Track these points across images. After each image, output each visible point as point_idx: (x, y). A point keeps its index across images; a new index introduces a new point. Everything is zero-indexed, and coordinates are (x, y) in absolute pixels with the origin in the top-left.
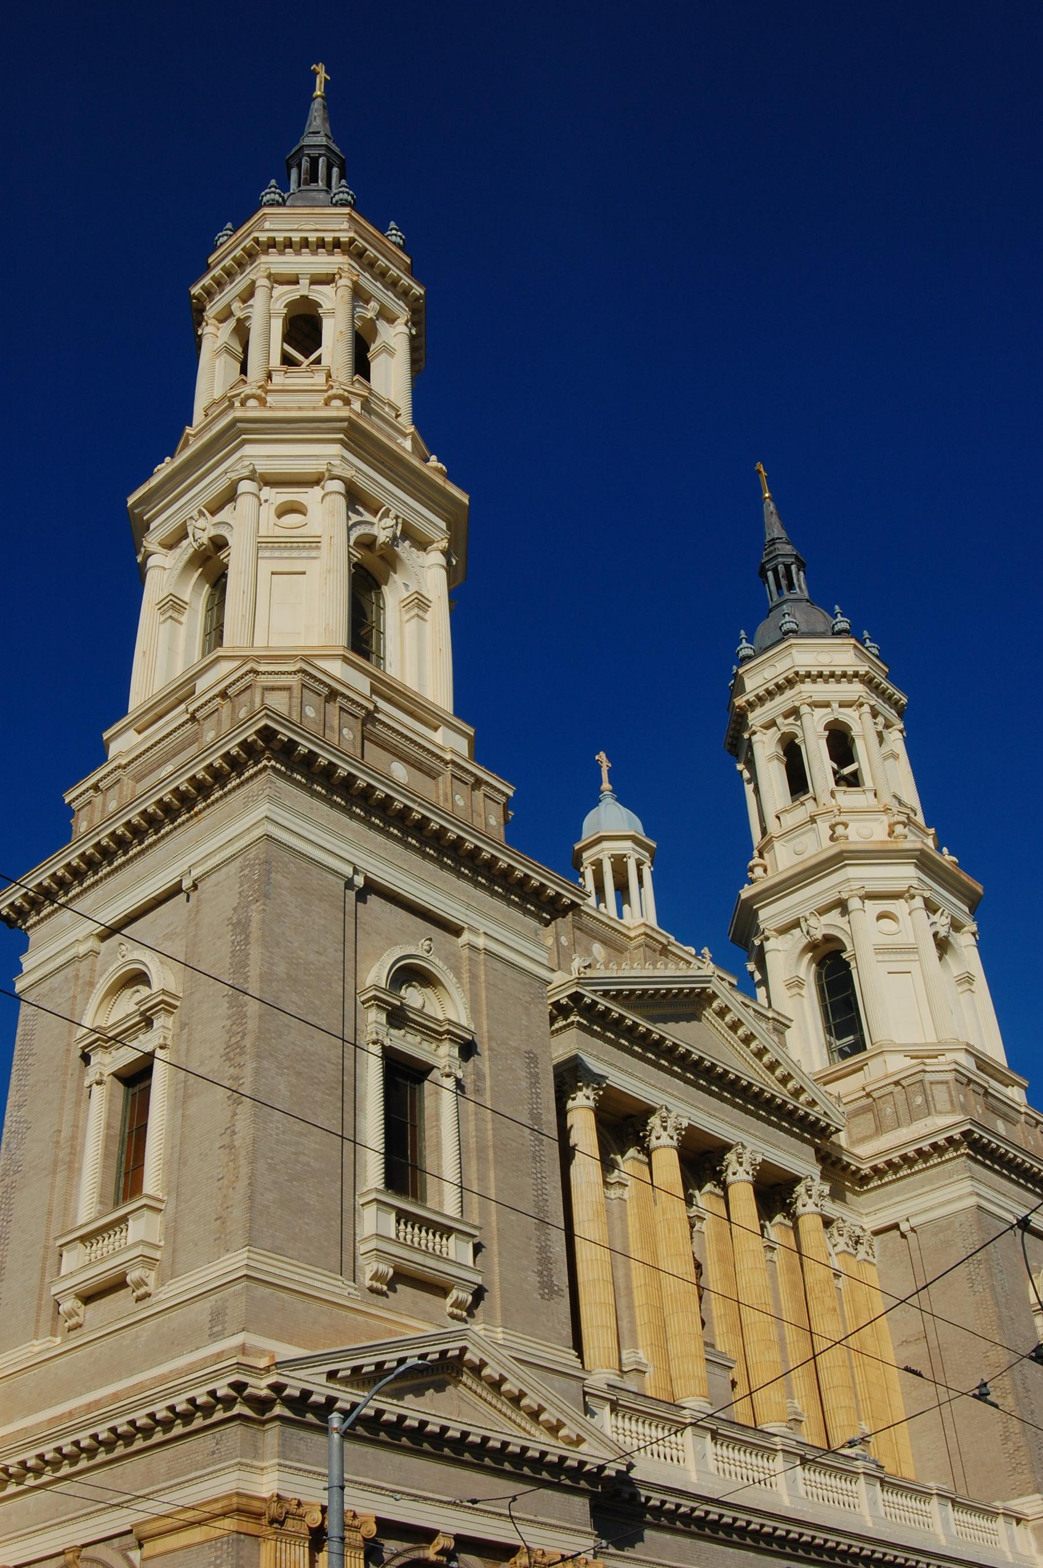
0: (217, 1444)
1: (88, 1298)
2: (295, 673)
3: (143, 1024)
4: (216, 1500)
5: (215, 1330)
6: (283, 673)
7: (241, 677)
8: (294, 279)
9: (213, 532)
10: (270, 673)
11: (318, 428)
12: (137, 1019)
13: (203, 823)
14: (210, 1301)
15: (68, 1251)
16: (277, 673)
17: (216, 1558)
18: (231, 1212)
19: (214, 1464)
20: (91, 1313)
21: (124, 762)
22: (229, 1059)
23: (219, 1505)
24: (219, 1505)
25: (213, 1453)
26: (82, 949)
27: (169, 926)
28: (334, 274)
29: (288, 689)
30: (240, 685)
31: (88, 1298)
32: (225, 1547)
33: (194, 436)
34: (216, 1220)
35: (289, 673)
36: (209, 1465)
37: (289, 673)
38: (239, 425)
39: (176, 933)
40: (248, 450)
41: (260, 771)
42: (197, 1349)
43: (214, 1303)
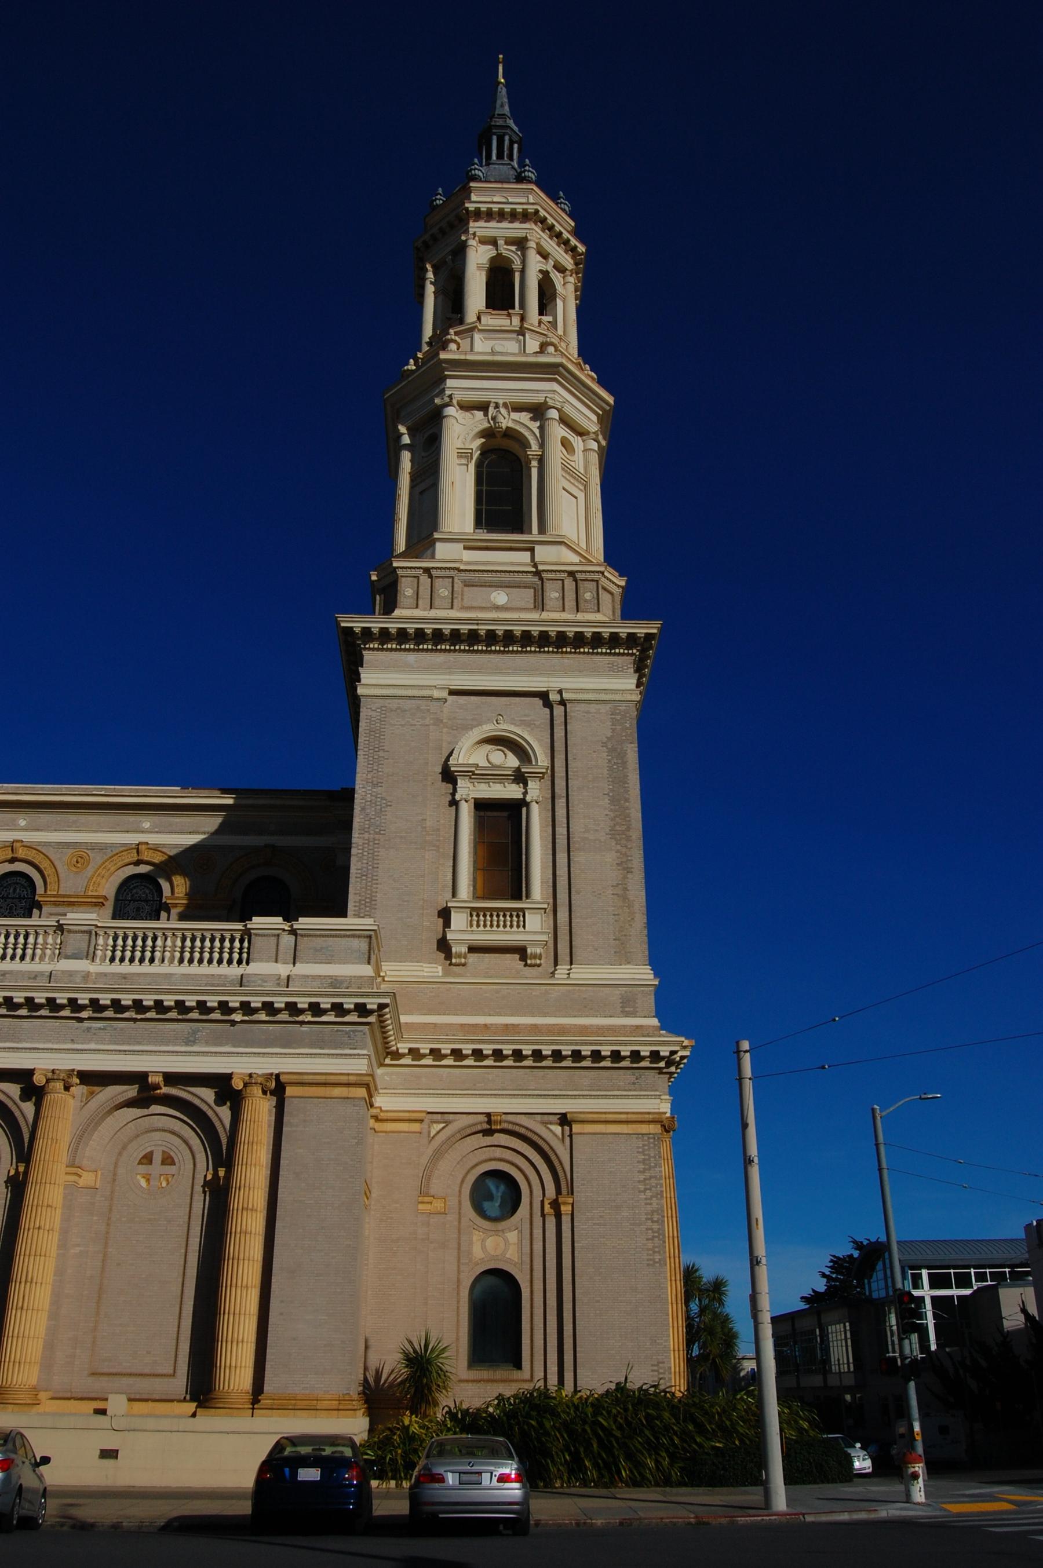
0: (637, 1079)
1: (472, 949)
2: (618, 586)
3: (513, 777)
4: (649, 1113)
5: (627, 1009)
6: (613, 583)
7: (593, 572)
8: (545, 254)
9: (511, 425)
10: (608, 579)
11: (595, 400)
12: (510, 773)
13: (566, 661)
14: (619, 990)
15: (455, 912)
16: (611, 581)
17: (644, 1145)
18: (630, 940)
19: (635, 1090)
20: (473, 958)
21: (462, 567)
22: (616, 839)
23: (651, 1116)
24: (651, 1116)
25: (634, 1083)
26: (436, 694)
27: (525, 715)
28: (567, 269)
29: (611, 594)
30: (588, 576)
31: (472, 949)
32: (652, 1140)
33: (479, 330)
34: (614, 940)
35: (616, 585)
36: (630, 1090)
37: (616, 585)
38: (561, 368)
39: (535, 724)
40: (555, 386)
41: (628, 654)
42: (611, 1017)
43: (623, 992)
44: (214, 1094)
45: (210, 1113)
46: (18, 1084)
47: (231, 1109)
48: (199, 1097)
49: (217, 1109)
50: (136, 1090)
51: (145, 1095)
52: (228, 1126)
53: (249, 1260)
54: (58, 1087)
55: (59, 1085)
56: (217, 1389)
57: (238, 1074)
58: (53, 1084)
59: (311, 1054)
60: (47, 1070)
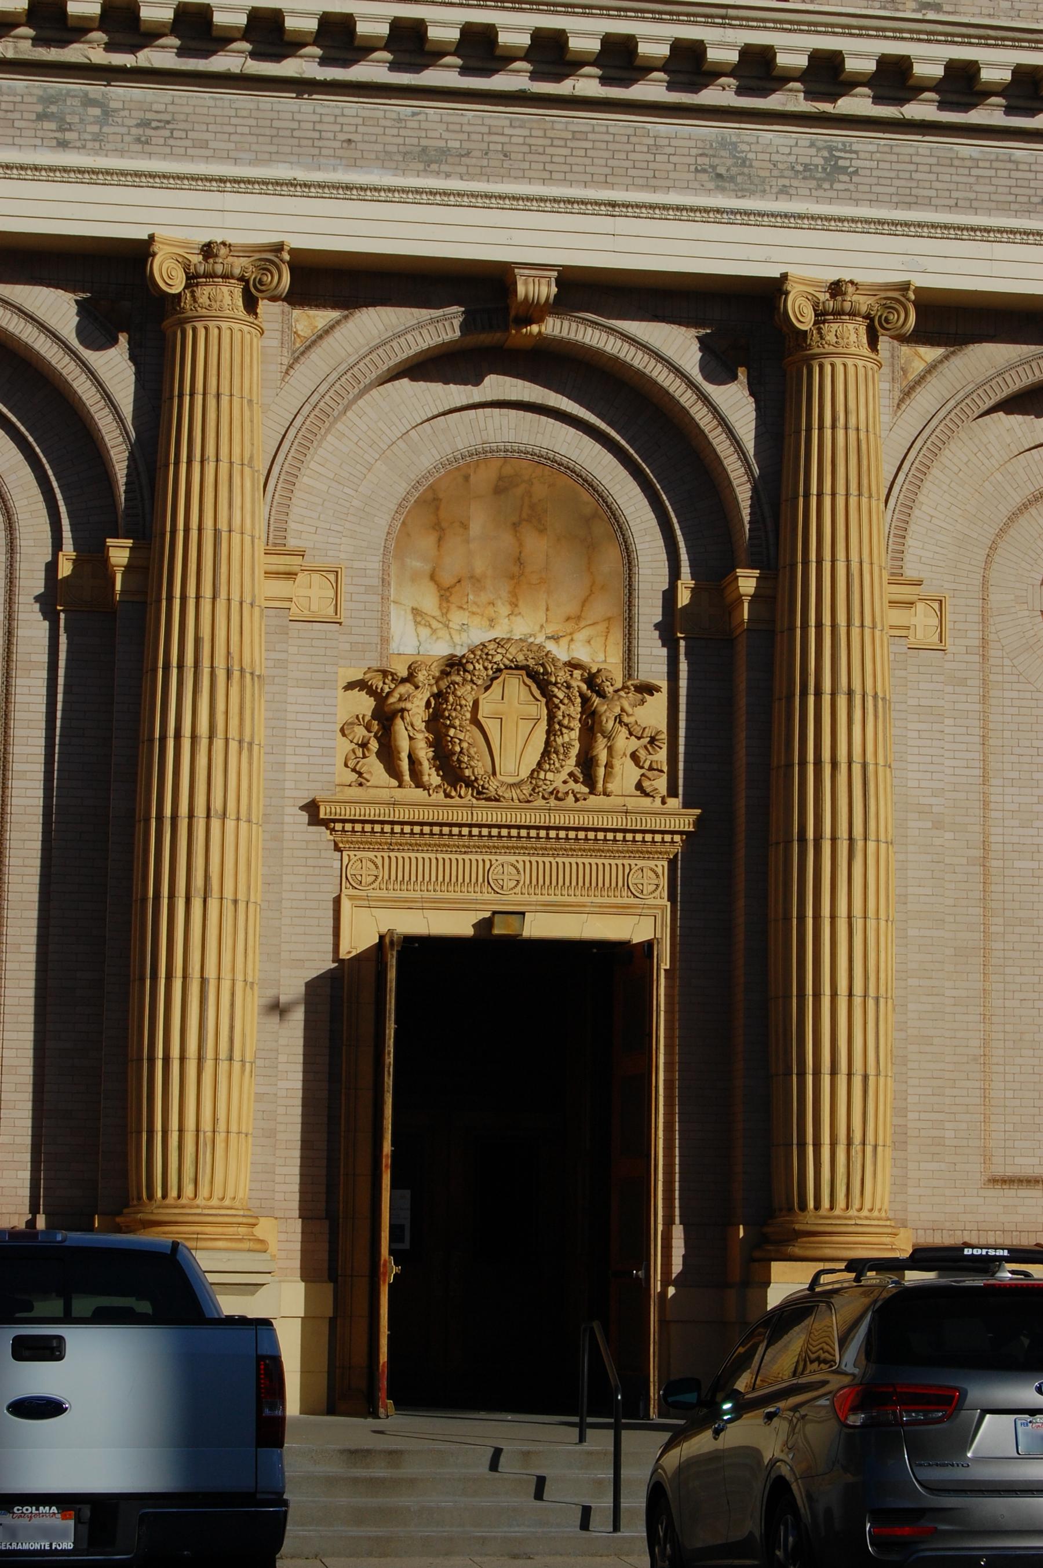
44: (74, 309)
45: (686, 398)
46: (74, 291)
47: (133, 358)
48: (30, 318)
49: (711, 389)
50: (457, 323)
51: (486, 338)
52: (127, 409)
53: (878, 841)
54: (227, 300)
55: (230, 296)
56: (811, 1204)
57: (804, 281)
58: (207, 290)
59: (946, 227)
60: (185, 244)
